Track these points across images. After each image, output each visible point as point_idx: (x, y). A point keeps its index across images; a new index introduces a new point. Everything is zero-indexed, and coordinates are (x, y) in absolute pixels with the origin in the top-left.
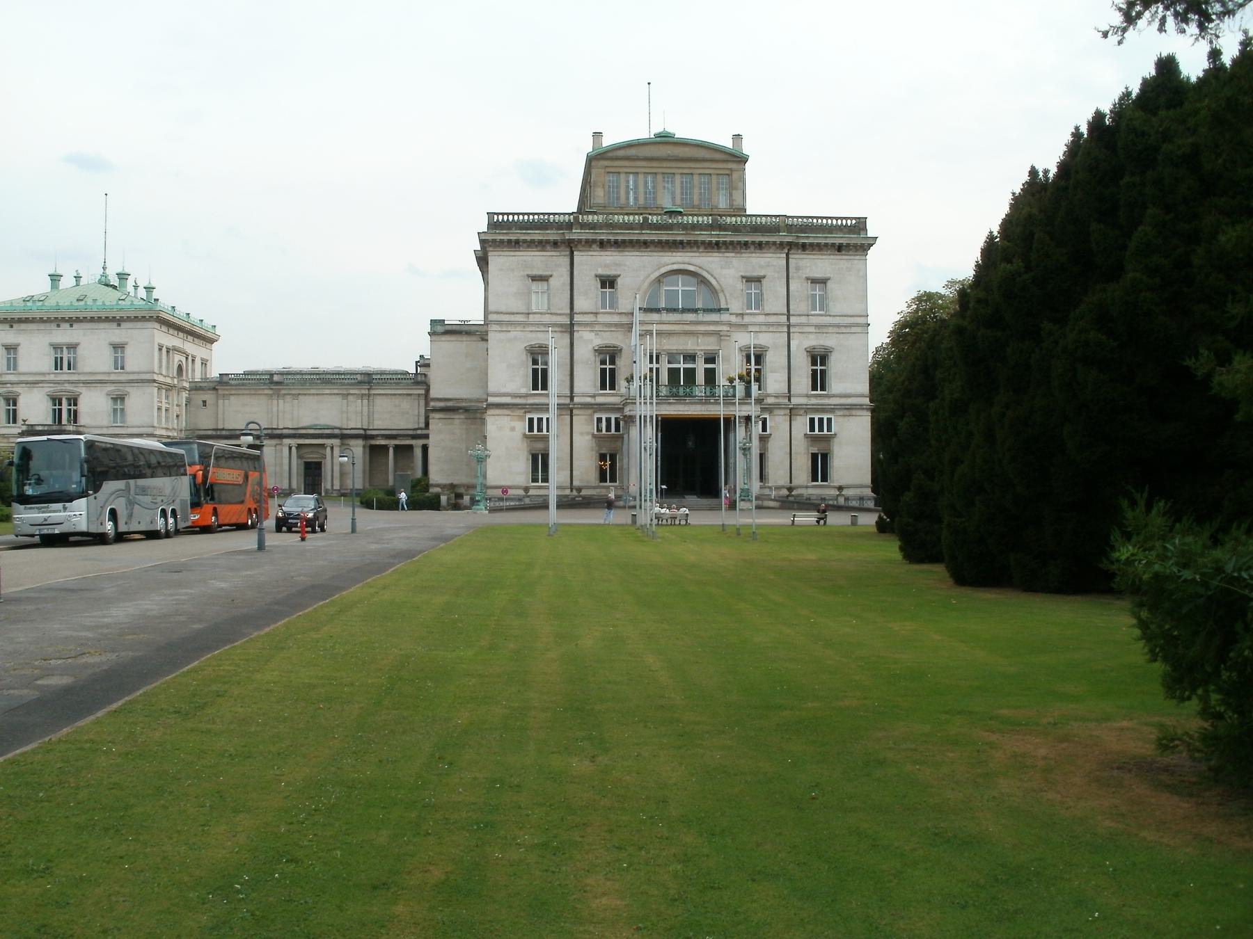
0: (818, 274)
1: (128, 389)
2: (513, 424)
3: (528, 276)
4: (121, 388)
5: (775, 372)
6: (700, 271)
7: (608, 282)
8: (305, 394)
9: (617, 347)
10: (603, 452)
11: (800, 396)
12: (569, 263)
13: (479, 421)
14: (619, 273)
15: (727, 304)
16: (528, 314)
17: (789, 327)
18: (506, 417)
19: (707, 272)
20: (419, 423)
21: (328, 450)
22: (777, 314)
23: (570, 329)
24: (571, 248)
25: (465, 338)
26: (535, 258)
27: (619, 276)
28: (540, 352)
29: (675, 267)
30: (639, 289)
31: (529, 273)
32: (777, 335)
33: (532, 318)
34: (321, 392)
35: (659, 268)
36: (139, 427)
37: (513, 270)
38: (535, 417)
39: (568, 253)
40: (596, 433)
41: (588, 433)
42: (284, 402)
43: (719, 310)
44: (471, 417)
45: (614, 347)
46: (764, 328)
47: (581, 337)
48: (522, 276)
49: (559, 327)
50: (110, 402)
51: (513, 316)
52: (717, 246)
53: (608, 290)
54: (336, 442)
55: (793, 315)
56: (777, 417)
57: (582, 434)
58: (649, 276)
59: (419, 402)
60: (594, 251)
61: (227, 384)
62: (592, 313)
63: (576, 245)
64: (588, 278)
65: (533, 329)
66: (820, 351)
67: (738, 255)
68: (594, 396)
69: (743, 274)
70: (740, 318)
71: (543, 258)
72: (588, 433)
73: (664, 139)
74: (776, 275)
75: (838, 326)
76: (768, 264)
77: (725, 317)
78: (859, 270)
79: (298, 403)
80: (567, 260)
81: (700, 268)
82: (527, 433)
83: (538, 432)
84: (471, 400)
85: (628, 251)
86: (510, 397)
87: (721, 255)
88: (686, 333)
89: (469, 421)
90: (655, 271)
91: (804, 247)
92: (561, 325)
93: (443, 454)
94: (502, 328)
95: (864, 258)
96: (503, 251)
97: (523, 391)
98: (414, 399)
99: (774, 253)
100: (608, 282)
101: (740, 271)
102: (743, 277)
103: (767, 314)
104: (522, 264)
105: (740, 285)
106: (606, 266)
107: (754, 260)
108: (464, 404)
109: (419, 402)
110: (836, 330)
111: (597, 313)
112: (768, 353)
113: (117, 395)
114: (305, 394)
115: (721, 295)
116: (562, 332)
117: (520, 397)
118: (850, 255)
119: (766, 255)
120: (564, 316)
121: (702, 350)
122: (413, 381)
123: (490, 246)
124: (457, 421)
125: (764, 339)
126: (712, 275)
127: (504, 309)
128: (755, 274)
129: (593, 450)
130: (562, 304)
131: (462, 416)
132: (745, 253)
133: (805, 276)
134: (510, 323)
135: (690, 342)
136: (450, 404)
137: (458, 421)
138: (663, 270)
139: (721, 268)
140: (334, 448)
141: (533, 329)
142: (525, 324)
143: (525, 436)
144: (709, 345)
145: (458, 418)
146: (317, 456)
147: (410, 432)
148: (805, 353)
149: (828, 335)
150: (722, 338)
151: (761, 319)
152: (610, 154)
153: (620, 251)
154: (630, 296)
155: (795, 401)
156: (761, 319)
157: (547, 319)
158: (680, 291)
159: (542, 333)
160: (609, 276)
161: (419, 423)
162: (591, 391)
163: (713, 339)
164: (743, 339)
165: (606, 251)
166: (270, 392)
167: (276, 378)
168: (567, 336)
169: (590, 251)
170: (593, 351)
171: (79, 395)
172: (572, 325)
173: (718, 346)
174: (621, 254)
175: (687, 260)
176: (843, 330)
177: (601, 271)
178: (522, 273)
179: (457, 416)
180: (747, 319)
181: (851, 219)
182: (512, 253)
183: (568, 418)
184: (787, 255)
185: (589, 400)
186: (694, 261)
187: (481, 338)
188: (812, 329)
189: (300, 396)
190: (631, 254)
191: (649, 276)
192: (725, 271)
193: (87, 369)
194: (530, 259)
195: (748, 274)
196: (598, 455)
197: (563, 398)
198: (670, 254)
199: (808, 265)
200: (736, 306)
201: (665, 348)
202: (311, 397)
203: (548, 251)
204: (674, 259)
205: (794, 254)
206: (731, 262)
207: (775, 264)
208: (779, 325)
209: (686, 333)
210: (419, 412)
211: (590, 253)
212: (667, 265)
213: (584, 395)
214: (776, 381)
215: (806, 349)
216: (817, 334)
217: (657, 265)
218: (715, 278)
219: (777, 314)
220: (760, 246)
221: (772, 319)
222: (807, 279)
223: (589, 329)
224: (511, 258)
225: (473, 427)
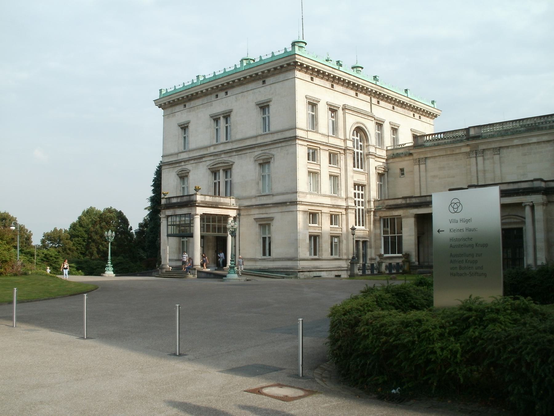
1: (273, 152)
4: (267, 151)
8: (507, 147)
21: (528, 209)
34: (526, 141)
36: (283, 194)
42: (484, 159)
50: (258, 168)
54: (538, 198)
61: (422, 146)
79: (500, 158)
113: (263, 159)
114: (507, 147)
140: (536, 208)
146: (515, 220)
166: (467, 149)
167: (472, 133)
171: (232, 165)
189: (501, 150)
193: (239, 137)
202: (515, 150)
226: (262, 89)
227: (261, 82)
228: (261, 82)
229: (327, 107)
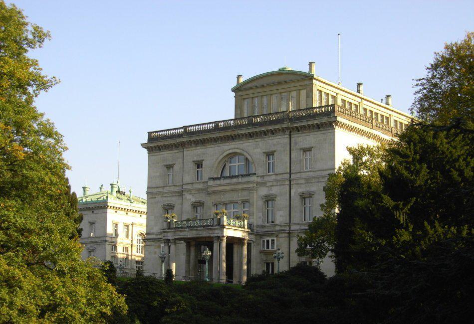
0: (306, 146)
2: (156, 250)
5: (280, 210)
6: (242, 152)
7: (199, 165)
11: (295, 224)
14: (202, 159)
17: (290, 181)
22: (282, 174)
27: (203, 160)
29: (231, 151)
31: (165, 164)
33: (167, 189)
35: (223, 153)
37: (158, 163)
45: (200, 202)
46: (275, 183)
47: (186, 198)
51: (157, 189)
52: (251, 136)
55: (293, 173)
56: (281, 239)
64: (190, 164)
65: (166, 195)
67: (262, 140)
69: (264, 151)
73: (282, 73)
76: (279, 142)
78: (331, 139)
81: (243, 150)
87: (253, 141)
88: (233, 190)
90: (222, 154)
91: (298, 129)
99: (280, 136)
100: (199, 165)
102: (264, 153)
107: (270, 142)
110: (317, 180)
111: (193, 183)
118: (325, 130)
119: (277, 137)
125: (275, 190)
138: (225, 154)
139: (254, 149)
141: (166, 195)
151: (273, 177)
152: (244, 87)
154: (206, 173)
155: (293, 227)
156: (273, 177)
163: (246, 193)
164: (263, 191)
175: (236, 146)
177: (195, 159)
178: (162, 164)
182: (158, 154)
184: (290, 135)
186: (241, 146)
188: (303, 181)
192: (255, 150)
195: (266, 151)
198: (228, 144)
199: (302, 140)
200: (261, 171)
204: (230, 147)
205: (293, 134)
207: (282, 142)
208: (283, 180)
209: (233, 190)
212: (227, 151)
214: (281, 216)
215: (299, 194)
218: (250, 155)
219: (282, 174)
220: (273, 132)
221: (280, 177)
222: (301, 149)
224: (157, 156)
226: (92, 215)
227: (91, 211)
228: (91, 211)
229: (123, 225)
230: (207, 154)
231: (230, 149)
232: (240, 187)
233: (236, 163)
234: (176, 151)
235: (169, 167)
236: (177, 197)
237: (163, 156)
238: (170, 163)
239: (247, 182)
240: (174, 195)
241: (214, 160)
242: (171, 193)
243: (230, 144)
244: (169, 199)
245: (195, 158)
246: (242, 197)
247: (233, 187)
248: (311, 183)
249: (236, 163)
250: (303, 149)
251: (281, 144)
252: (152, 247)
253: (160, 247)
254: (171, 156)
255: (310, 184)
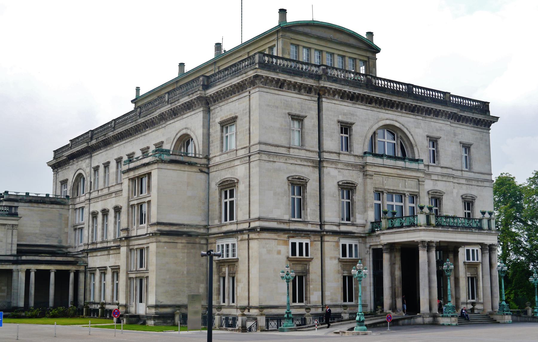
0: (465, 140)
3: (289, 114)
6: (402, 128)
9: (354, 184)
10: (345, 275)
12: (317, 107)
13: (198, 246)
15: (419, 156)
16: (289, 148)
18: (274, 241)
19: (407, 129)
20: (11, 250)
23: (319, 165)
24: (319, 94)
25: (187, 168)
26: (294, 99)
28: (299, 183)
29: (388, 122)
30: (366, 137)
32: (448, 183)
35: (378, 122)
37: (277, 107)
38: (297, 241)
39: (316, 99)
40: (341, 257)
41: (335, 258)
43: (417, 161)
44: (191, 242)
46: (440, 178)
47: (329, 173)
48: (285, 114)
49: (311, 162)
51: (278, 148)
53: (344, 135)
57: (331, 258)
58: (372, 127)
59: (12, 232)
60: (336, 100)
62: (336, 153)
63: (324, 94)
66: (469, 199)
67: (424, 119)
68: (339, 225)
70: (426, 168)
71: (299, 101)
72: (335, 258)
74: (445, 138)
75: (477, 180)
77: (421, 166)
80: (316, 105)
81: (403, 125)
82: (290, 256)
83: (299, 256)
84: (191, 226)
85: (359, 104)
86: (276, 223)
87: (414, 117)
88: (400, 176)
89: (190, 245)
92: (313, 161)
93: (168, 277)
94: (269, 158)
95: (488, 131)
96: (269, 88)
97: (287, 217)
98: (8, 229)
99: (443, 120)
101: (426, 132)
102: (428, 136)
103: (442, 167)
104: (284, 103)
105: (426, 143)
106: (345, 114)
108: (185, 230)
109: (12, 232)
112: (443, 197)
115: (415, 148)
116: (313, 167)
117: (284, 223)
120: (315, 154)
121: (408, 191)
122: (8, 213)
123: (261, 83)
124: (179, 246)
125: (440, 186)
126: (410, 132)
127: (270, 141)
128: (435, 134)
129: (339, 273)
130: (312, 142)
131: (184, 241)
132: (428, 118)
133: (459, 141)
134: (276, 154)
135: (400, 184)
136: (174, 228)
137: (181, 245)
139: (415, 127)
142: (287, 157)
143: (288, 258)
144: (412, 188)
145: (182, 241)
147: (11, 258)
148: (461, 199)
149: (473, 187)
150: (420, 183)
151: (439, 170)
153: (354, 103)
157: (303, 154)
158: (386, 142)
159: (299, 166)
160: (347, 123)
161: (11, 250)
162: (337, 220)
164: (429, 185)
165: (345, 101)
168: (317, 170)
169: (334, 99)
170: (338, 186)
172: (320, 162)
173: (417, 189)
174: (354, 106)
175: (395, 117)
176: (480, 184)
177: (341, 118)
178: (284, 111)
179: (180, 241)
180: (431, 169)
181: (478, 101)
182: (277, 92)
183: (320, 243)
185: (335, 228)
187: (199, 170)
188: (463, 181)
190: (360, 107)
191: (372, 127)
192: (417, 130)
194: (289, 99)
196: (342, 277)
197: (315, 225)
198: (384, 111)
199: (460, 132)
201: (386, 187)
203: (302, 95)
206: (420, 124)
207: (444, 128)
209: (400, 176)
210: (12, 241)
211: (334, 102)
212: (383, 120)
213: (332, 224)
215: (462, 196)
216: (468, 186)
217: (377, 119)
218: (412, 135)
222: (461, 143)
223: (334, 166)
225: (192, 251)
230: (356, 116)
231: (387, 119)
232: (408, 173)
233: (388, 139)
234: (306, 97)
235: (299, 119)
236: (311, 169)
237: (285, 98)
238: (297, 113)
239: (418, 170)
240: (306, 163)
241: (368, 128)
242: (301, 159)
243: (387, 112)
244: (298, 168)
245: (340, 116)
246: (409, 188)
247: (399, 172)
248: (472, 185)
249: (388, 139)
250: (463, 144)
251: (444, 130)
252: (274, 243)
253: (288, 245)
254: (298, 103)
255: (471, 186)
